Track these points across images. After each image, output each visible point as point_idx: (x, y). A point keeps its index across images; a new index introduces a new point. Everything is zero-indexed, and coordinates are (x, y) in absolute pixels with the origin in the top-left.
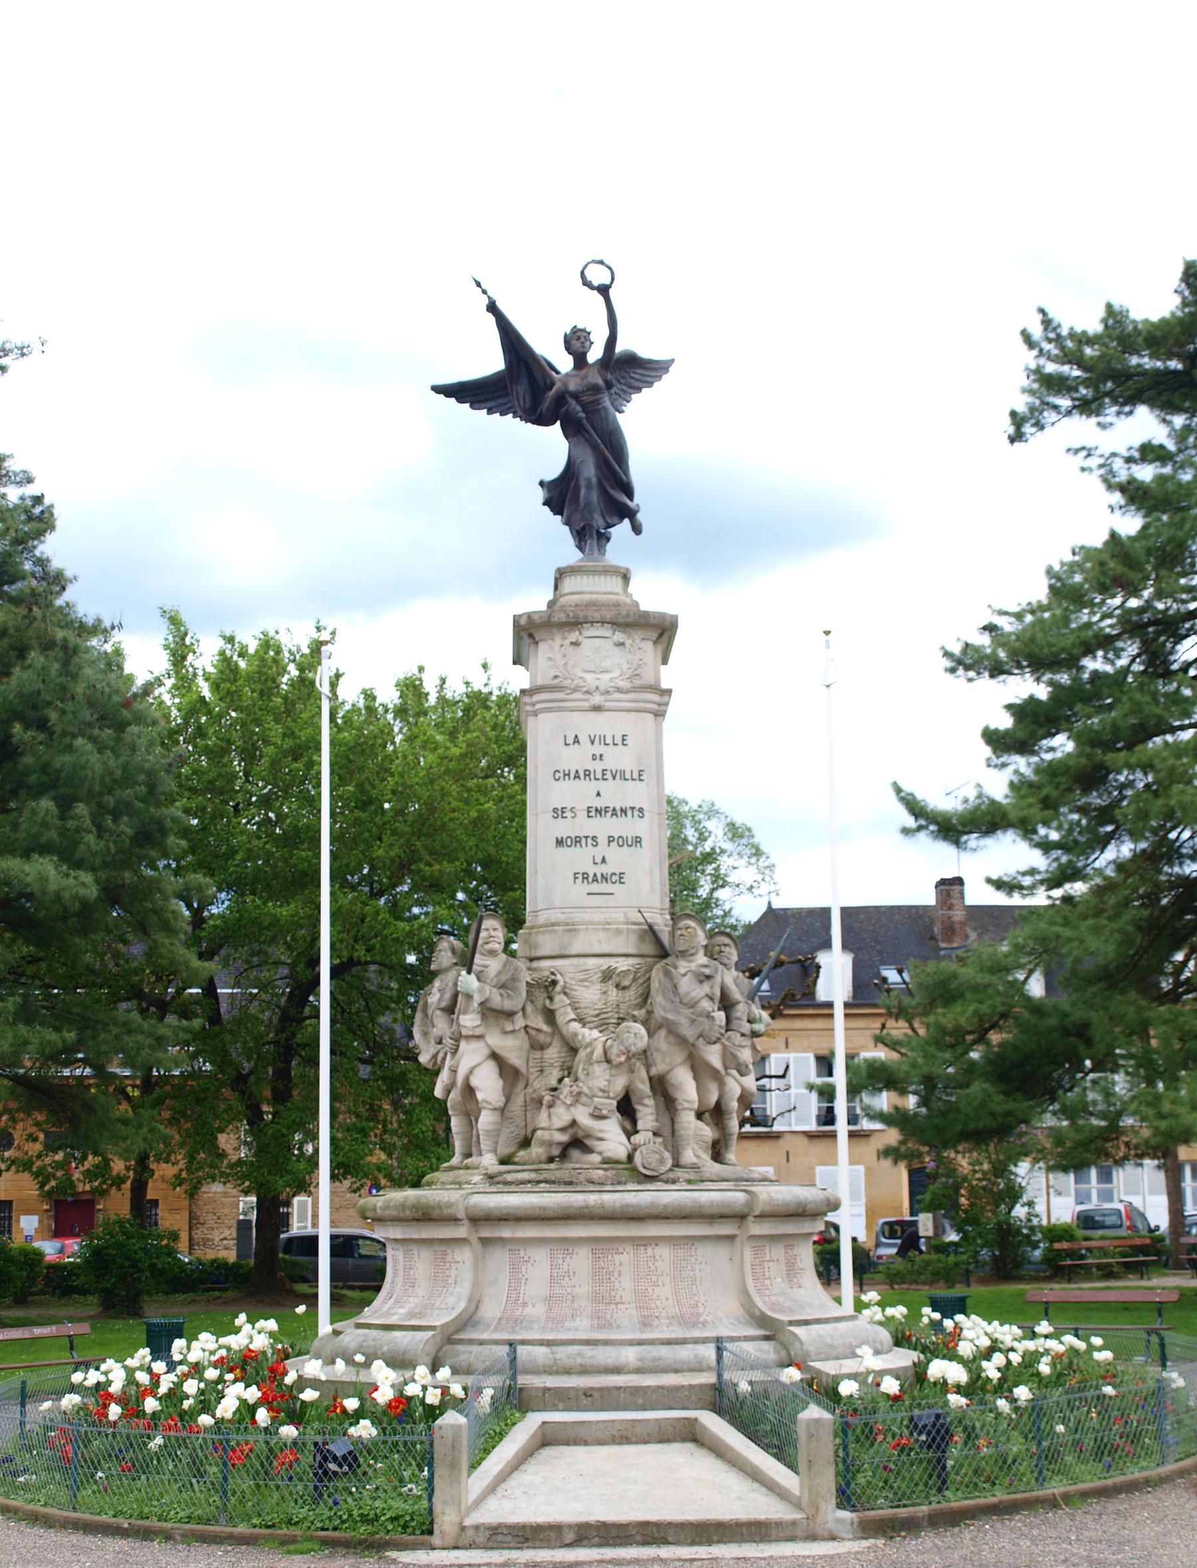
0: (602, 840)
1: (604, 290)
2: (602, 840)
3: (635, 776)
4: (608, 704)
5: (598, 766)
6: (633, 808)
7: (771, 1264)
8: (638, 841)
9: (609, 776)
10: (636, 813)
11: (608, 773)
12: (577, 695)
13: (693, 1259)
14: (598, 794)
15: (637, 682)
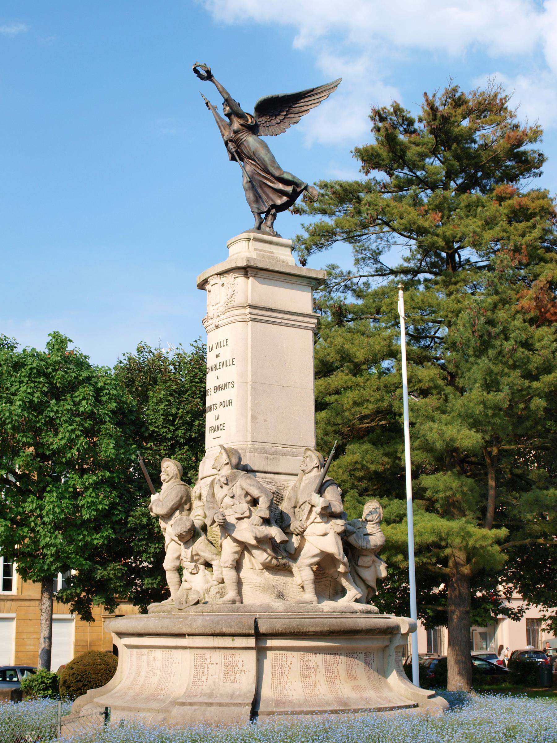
0: (218, 406)
1: (209, 76)
2: (218, 406)
3: (231, 363)
4: (220, 323)
5: (217, 361)
6: (229, 383)
7: (210, 666)
8: (230, 402)
9: (221, 366)
10: (231, 385)
11: (221, 364)
12: (210, 321)
13: (172, 660)
14: (218, 378)
15: (231, 305)
